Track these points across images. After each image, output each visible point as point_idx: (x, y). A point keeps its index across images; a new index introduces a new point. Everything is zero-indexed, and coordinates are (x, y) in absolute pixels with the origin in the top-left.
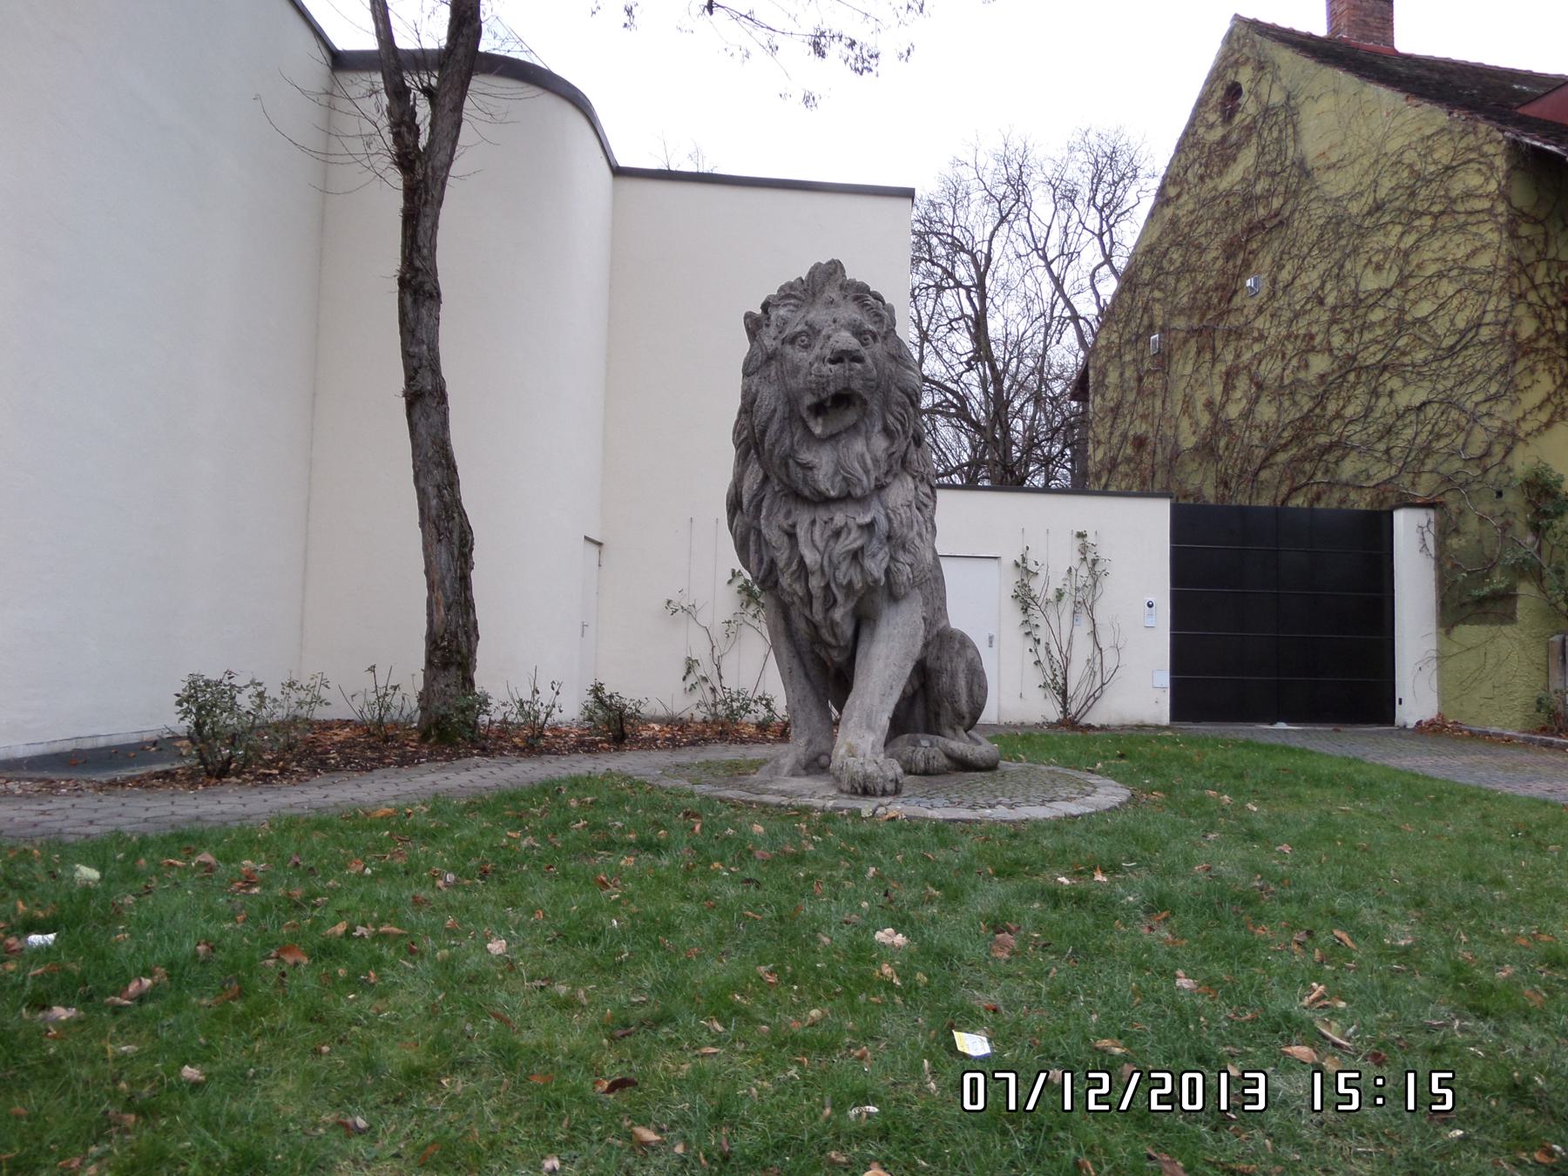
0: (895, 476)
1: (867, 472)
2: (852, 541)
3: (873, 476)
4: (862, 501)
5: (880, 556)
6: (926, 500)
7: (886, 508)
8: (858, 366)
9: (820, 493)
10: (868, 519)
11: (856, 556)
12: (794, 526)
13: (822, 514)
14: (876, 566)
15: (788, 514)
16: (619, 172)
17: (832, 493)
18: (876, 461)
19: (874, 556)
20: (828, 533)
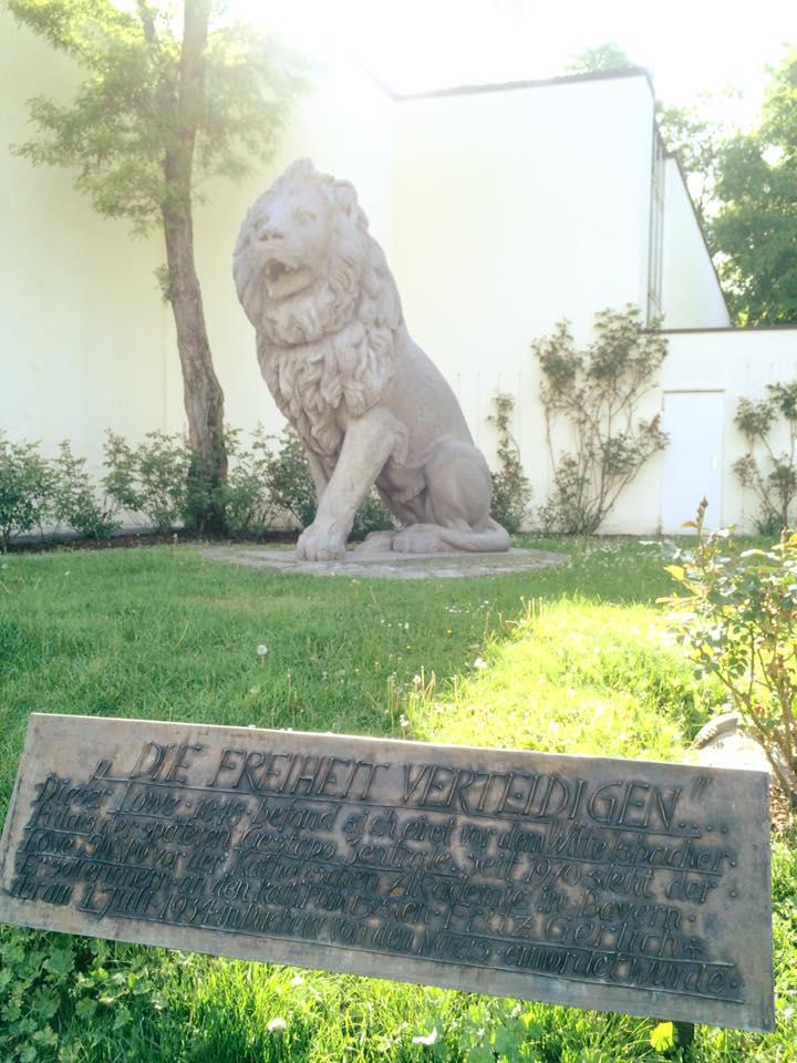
0: (346, 324)
1: (313, 322)
2: (311, 374)
3: (318, 325)
4: (316, 342)
5: (332, 385)
6: (379, 341)
7: (334, 348)
8: (278, 241)
9: (286, 342)
10: (318, 357)
11: (318, 384)
12: (278, 367)
13: (292, 355)
14: (330, 394)
15: (277, 359)
16: (397, 98)
17: (291, 340)
18: (320, 314)
19: (326, 386)
20: (295, 370)
